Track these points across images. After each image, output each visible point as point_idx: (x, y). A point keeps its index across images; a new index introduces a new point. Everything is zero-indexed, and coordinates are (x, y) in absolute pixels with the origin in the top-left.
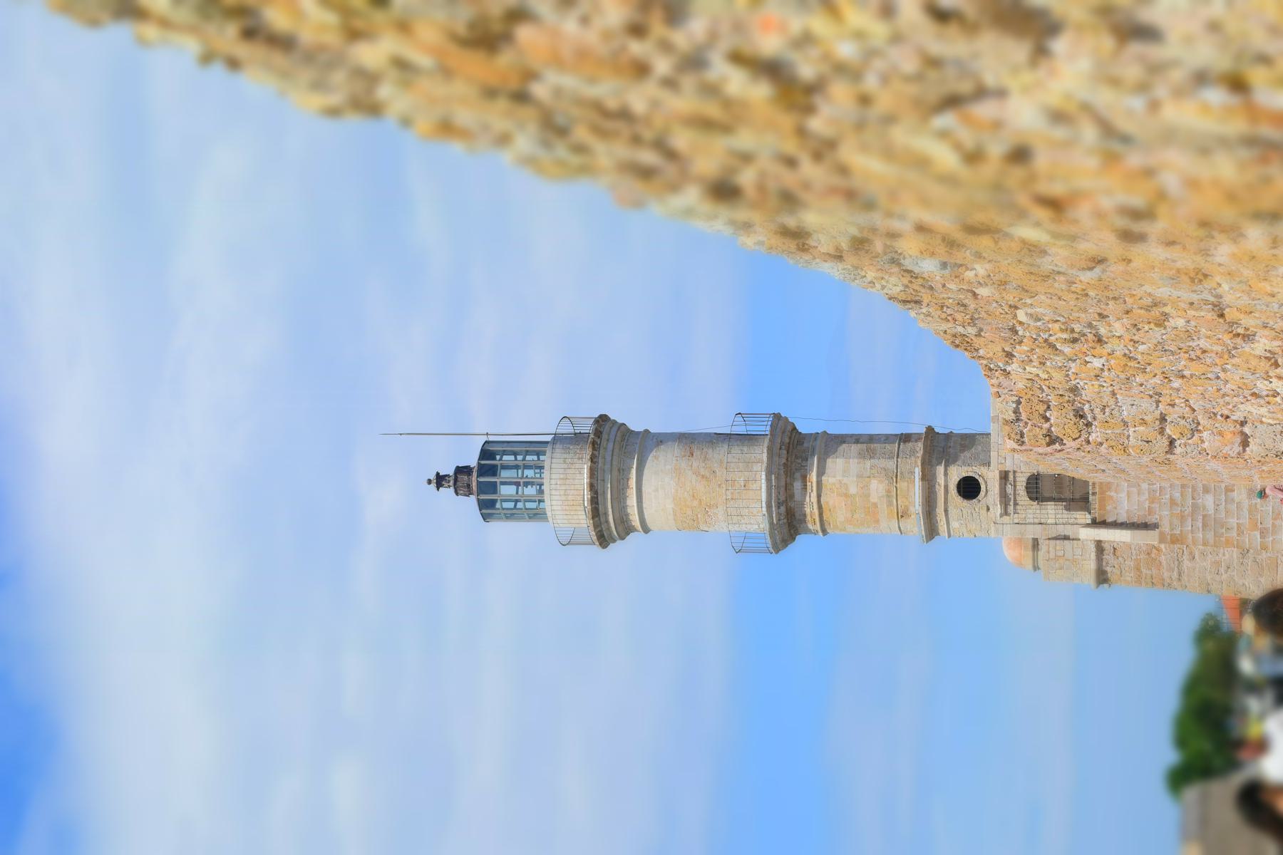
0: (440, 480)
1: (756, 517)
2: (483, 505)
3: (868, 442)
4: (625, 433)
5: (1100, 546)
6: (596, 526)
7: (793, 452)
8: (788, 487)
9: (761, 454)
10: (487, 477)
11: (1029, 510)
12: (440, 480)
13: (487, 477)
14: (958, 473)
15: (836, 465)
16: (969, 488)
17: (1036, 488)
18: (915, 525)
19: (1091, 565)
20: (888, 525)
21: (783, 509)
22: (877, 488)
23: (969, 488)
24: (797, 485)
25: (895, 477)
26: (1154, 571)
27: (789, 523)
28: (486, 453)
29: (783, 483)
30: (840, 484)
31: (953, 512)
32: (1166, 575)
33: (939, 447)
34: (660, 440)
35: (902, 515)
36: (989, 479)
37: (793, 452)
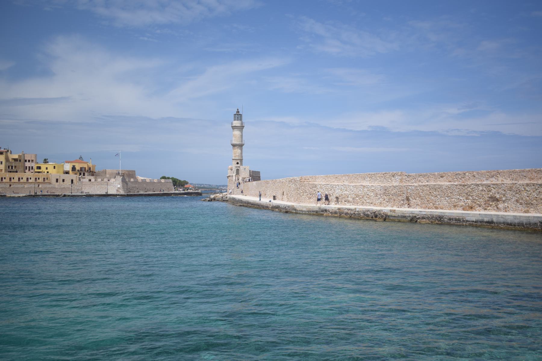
1: (235, 142)
3: (242, 153)
7: (241, 146)
11: (236, 169)
16: (238, 163)
17: (238, 170)
18: (234, 158)
20: (234, 155)
22: (238, 154)
23: (238, 163)
27: (234, 145)
30: (238, 151)
33: (241, 160)
34: (242, 133)
36: (239, 165)
37: (241, 146)
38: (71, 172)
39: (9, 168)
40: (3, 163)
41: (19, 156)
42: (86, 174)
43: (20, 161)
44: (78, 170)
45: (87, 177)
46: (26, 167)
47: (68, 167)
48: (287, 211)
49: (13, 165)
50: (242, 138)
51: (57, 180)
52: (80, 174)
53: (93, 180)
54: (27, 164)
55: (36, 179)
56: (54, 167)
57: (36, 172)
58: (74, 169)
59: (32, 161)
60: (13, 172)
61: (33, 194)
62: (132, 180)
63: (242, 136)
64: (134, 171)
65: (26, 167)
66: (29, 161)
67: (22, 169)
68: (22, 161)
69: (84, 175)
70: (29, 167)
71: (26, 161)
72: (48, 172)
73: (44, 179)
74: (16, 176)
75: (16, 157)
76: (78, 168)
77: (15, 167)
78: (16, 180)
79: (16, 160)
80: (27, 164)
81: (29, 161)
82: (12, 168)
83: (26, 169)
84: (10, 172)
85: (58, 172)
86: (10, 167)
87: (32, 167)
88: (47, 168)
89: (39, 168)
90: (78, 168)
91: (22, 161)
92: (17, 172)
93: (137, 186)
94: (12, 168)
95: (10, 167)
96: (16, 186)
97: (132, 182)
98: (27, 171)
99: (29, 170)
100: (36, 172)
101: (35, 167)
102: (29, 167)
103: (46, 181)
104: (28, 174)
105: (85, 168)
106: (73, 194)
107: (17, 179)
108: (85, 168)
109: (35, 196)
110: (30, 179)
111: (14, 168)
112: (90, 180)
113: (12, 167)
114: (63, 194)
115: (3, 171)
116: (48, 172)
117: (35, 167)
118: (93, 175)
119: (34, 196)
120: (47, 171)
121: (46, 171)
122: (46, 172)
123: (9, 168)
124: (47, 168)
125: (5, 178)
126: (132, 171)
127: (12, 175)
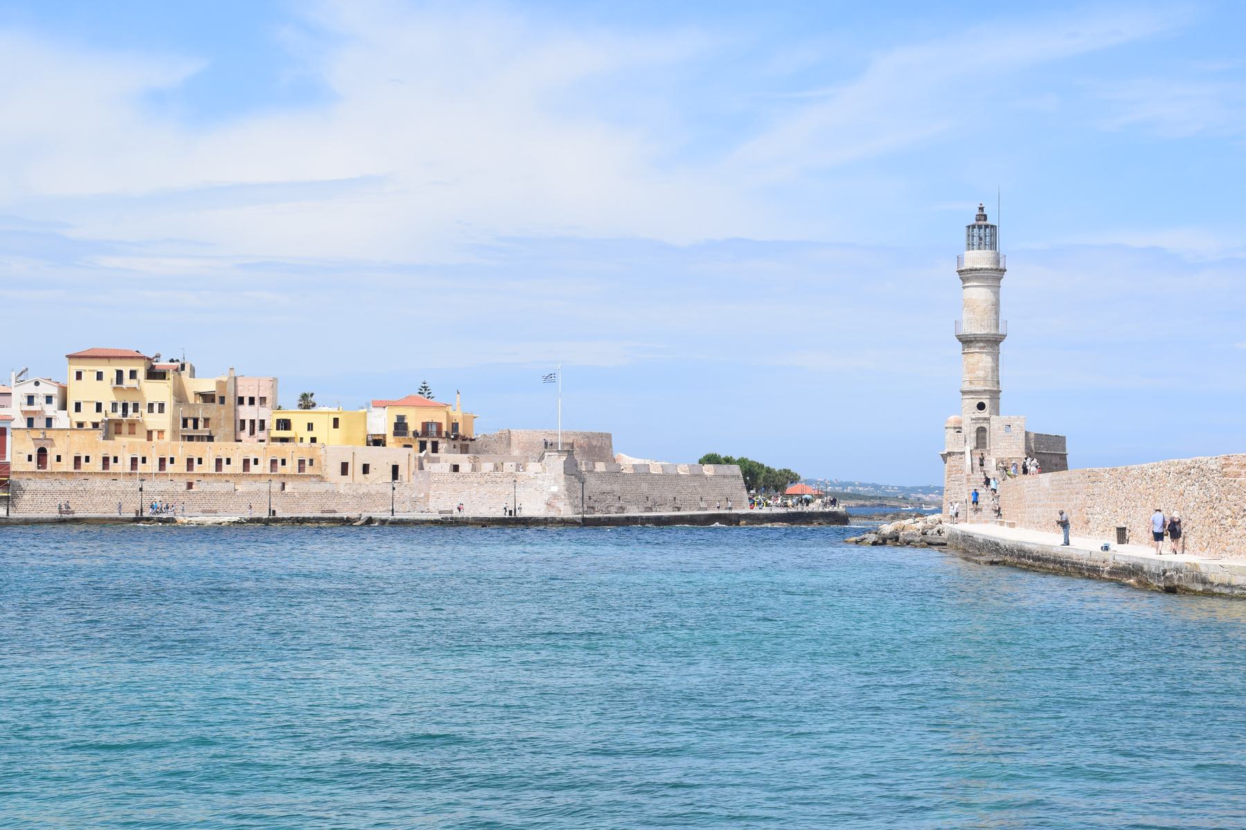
3: (996, 369)
4: (999, 279)
7: (994, 342)
9: (993, 332)
14: (987, 402)
15: (989, 359)
16: (981, 406)
17: (981, 432)
18: (967, 387)
20: (967, 377)
22: (981, 373)
23: (981, 406)
25: (985, 379)
30: (981, 360)
35: (971, 382)
37: (994, 342)
38: (390, 439)
39: (185, 425)
40: (168, 408)
41: (220, 384)
42: (442, 446)
43: (222, 400)
44: (416, 434)
45: (448, 455)
46: (243, 422)
47: (382, 423)
48: (1128, 576)
49: (201, 415)
50: (997, 313)
51: (344, 468)
52: (423, 446)
53: (465, 467)
54: (246, 412)
55: (274, 462)
56: (336, 423)
57: (274, 440)
58: (400, 427)
59: (263, 400)
60: (200, 438)
61: (265, 515)
62: (600, 467)
63: (996, 305)
64: (609, 436)
65: (243, 422)
66: (252, 401)
67: (230, 429)
68: (230, 400)
69: (435, 449)
70: (253, 422)
71: (241, 401)
72: (313, 440)
73: (301, 462)
74: (209, 452)
75: (209, 386)
76: (414, 425)
77: (206, 420)
78: (209, 466)
79: (207, 398)
80: (246, 412)
82: (196, 426)
83: (243, 428)
84: (190, 438)
85: (348, 440)
86: (190, 423)
87: (262, 422)
88: (310, 427)
89: (285, 424)
90: (414, 425)
91: (230, 400)
92: (210, 438)
93: (616, 487)
94: (196, 426)
95: (190, 423)
96: (208, 488)
97: (600, 476)
98: (245, 435)
99: (252, 432)
100: (274, 440)
101: (271, 424)
103: (308, 470)
104: (249, 446)
105: (439, 425)
106: (398, 516)
107: (213, 463)
108: (439, 425)
109: (272, 521)
110: (256, 462)
111: (201, 424)
112: (456, 468)
113: (196, 421)
114: (365, 516)
115: (167, 435)
117: (271, 424)
118: (465, 450)
119: (267, 522)
121: (307, 436)
122: (307, 440)
123: (185, 425)
124: (310, 427)
125: (172, 461)
126: (601, 435)
127: (196, 449)
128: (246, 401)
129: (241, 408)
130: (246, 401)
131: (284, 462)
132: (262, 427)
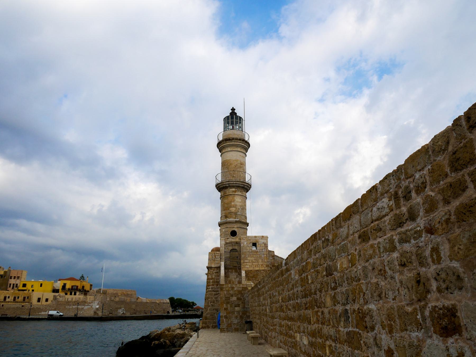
0: (233, 109)
2: (228, 117)
5: (219, 268)
6: (222, 141)
8: (233, 187)
10: (233, 119)
12: (233, 109)
13: (233, 119)
18: (224, 220)
19: (213, 266)
21: (227, 185)
23: (234, 234)
24: (234, 189)
26: (211, 283)
28: (240, 118)
29: (234, 185)
31: (227, 229)
32: (210, 287)
46: (10, 284)
54: (12, 281)
55: (15, 298)
59: (18, 277)
70: (14, 284)
71: (11, 278)
72: (33, 290)
73: (24, 298)
80: (12, 281)
81: (15, 277)
83: (10, 287)
87: (17, 284)
89: (24, 285)
99: (13, 288)
102: (14, 284)
110: (9, 297)
116: (33, 290)
120: (33, 289)
122: (31, 290)
128: (13, 278)
129: (10, 280)
130: (13, 278)
131: (18, 298)
132: (17, 286)
